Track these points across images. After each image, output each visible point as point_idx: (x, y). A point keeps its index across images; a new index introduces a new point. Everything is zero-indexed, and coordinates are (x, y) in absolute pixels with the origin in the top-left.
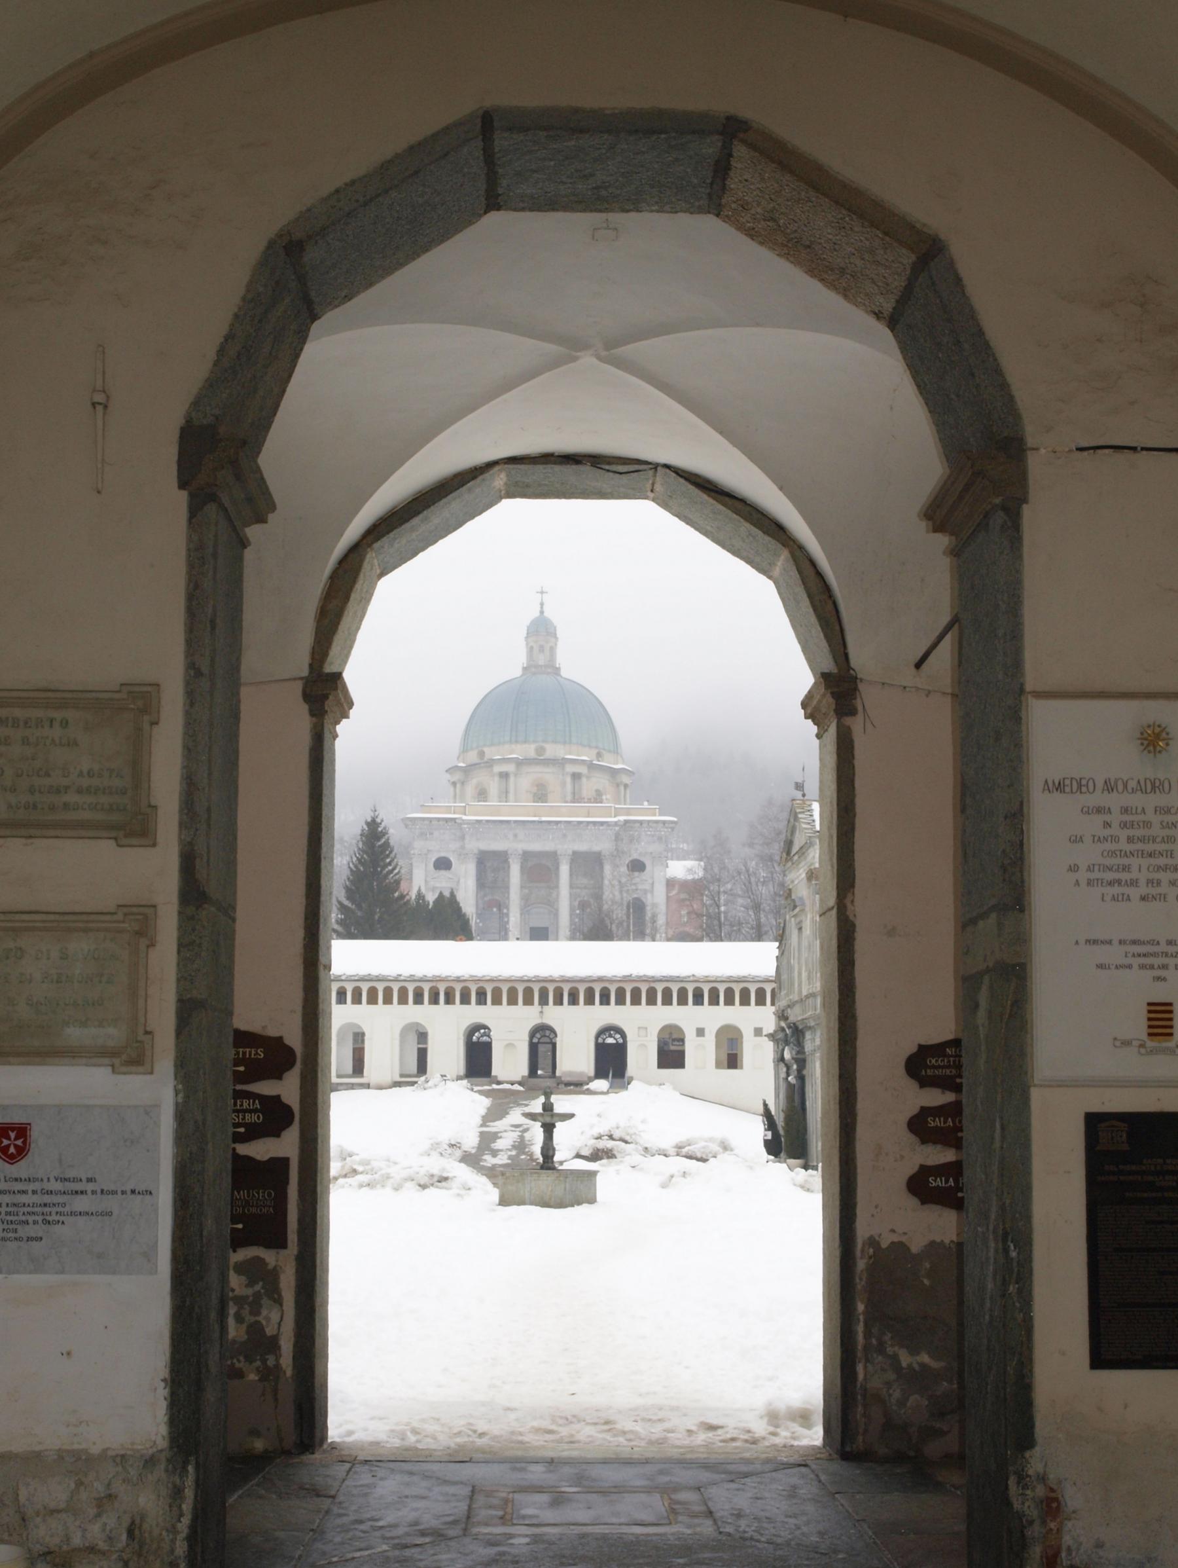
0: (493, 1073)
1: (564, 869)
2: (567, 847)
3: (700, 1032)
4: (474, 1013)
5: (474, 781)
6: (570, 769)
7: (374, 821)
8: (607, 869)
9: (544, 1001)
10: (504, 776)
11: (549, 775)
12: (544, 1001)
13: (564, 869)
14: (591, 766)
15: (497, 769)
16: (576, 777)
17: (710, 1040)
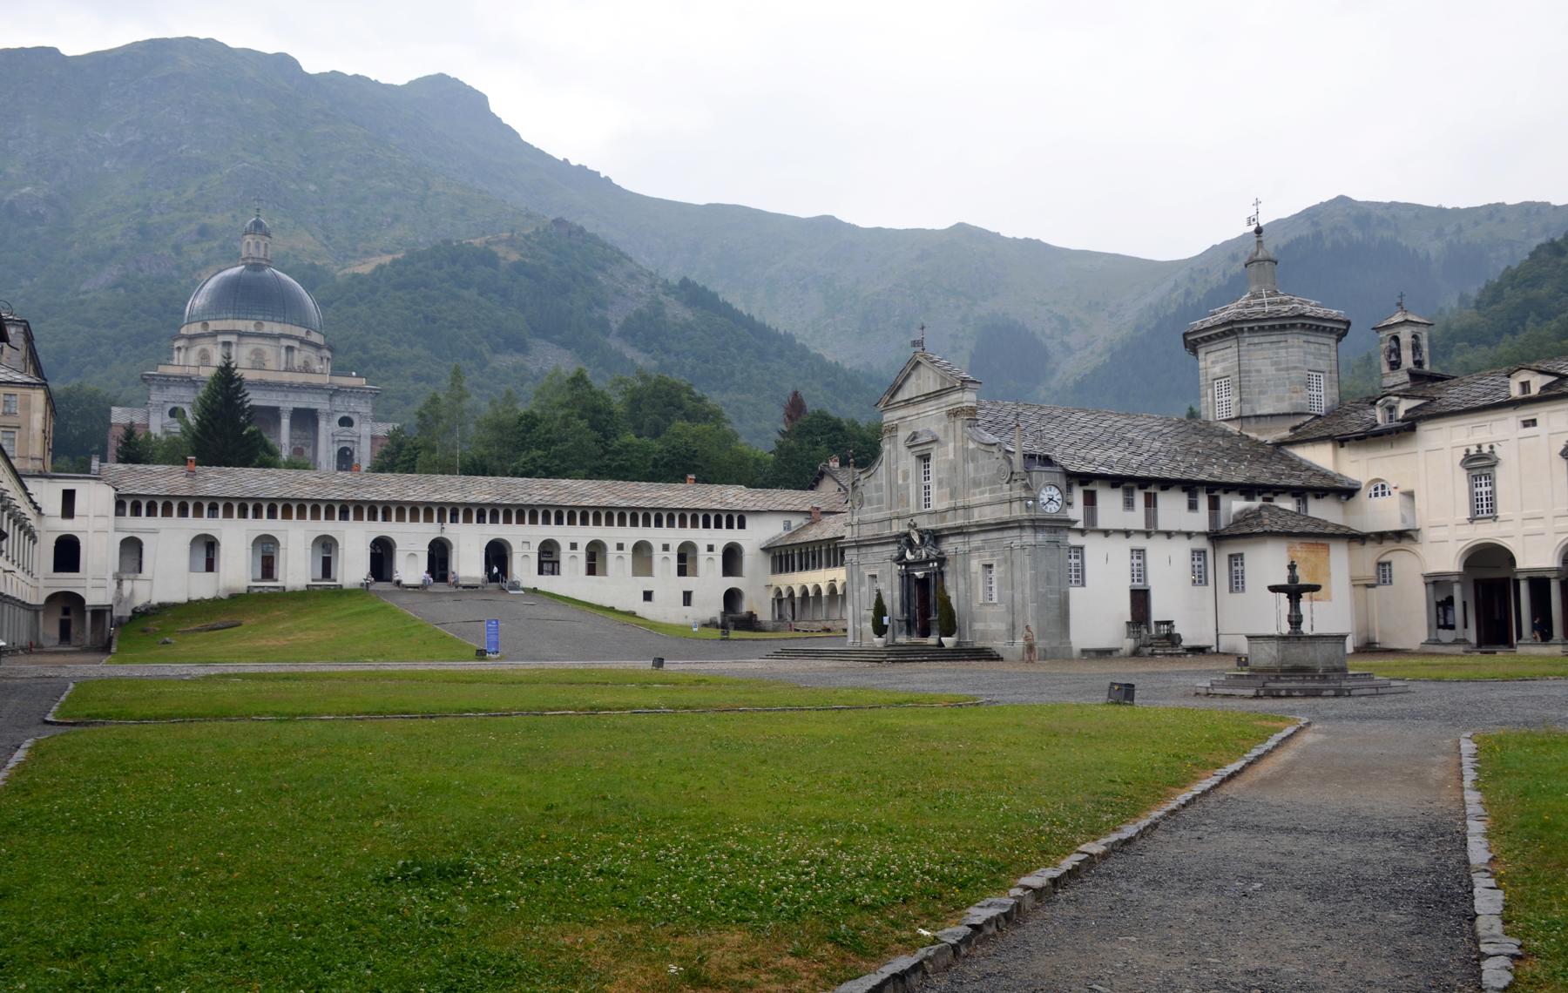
0: (396, 578)
1: (285, 422)
2: (288, 403)
3: (574, 546)
4: (380, 528)
5: (198, 348)
6: (285, 343)
7: (228, 365)
8: (322, 424)
9: (441, 519)
10: (227, 344)
11: (268, 347)
12: (441, 519)
13: (285, 422)
14: (303, 342)
15: (221, 338)
16: (290, 349)
17: (628, 551)
